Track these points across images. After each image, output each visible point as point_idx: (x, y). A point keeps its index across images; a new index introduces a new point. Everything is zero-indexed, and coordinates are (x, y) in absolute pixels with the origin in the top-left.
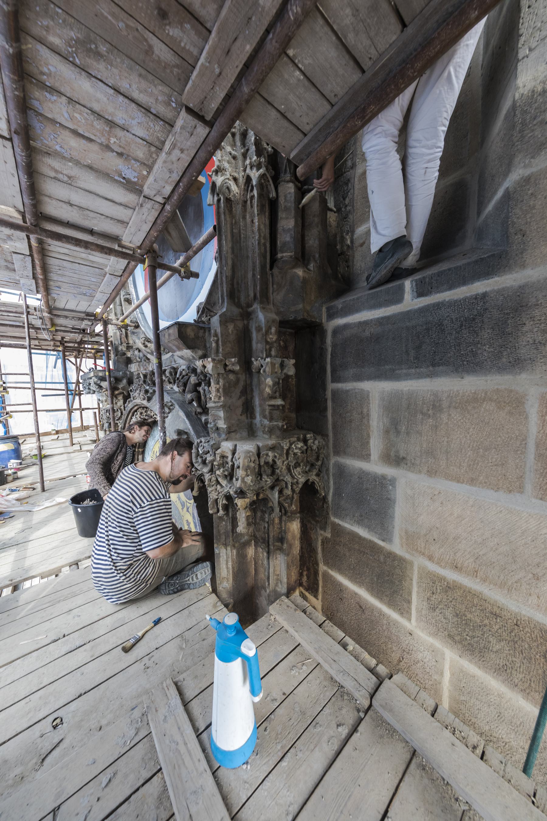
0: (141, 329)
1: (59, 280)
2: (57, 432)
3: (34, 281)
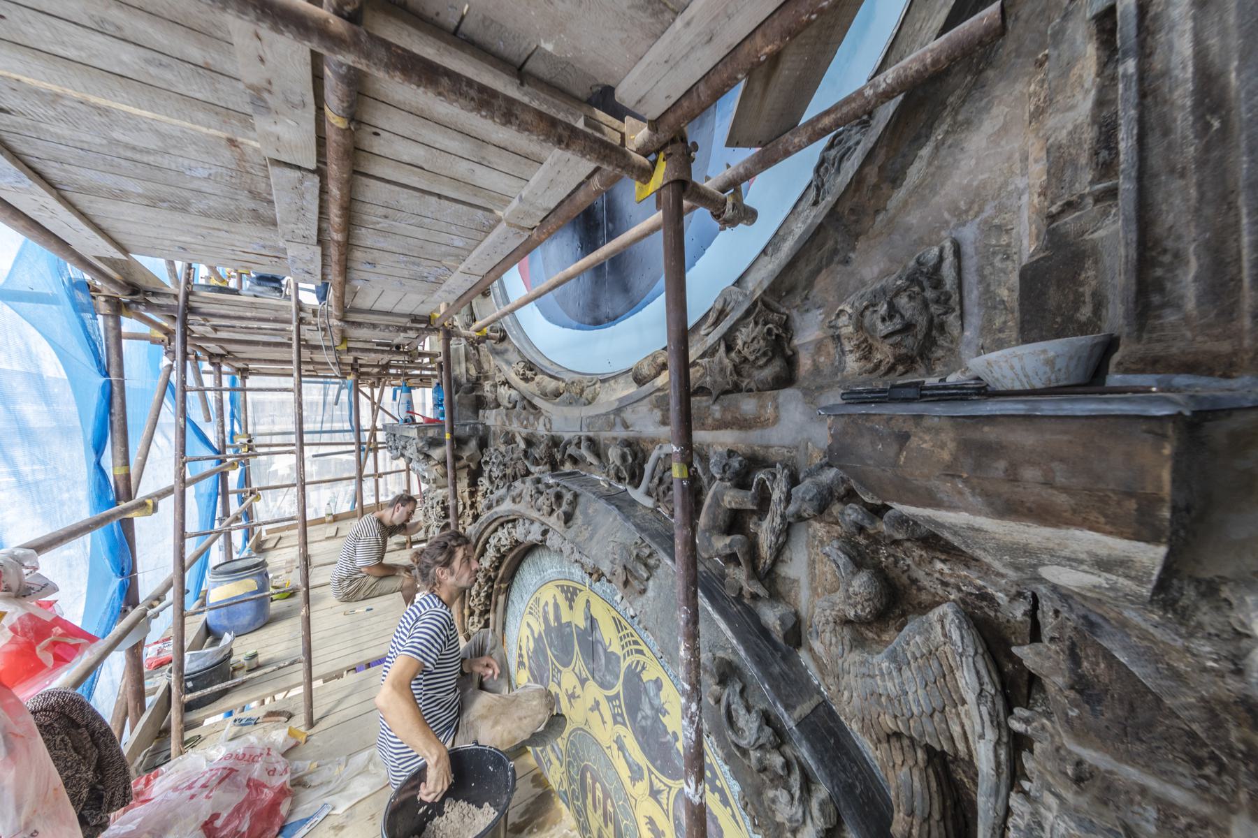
0: (511, 342)
1: (378, 245)
2: (336, 518)
3: (318, 250)
